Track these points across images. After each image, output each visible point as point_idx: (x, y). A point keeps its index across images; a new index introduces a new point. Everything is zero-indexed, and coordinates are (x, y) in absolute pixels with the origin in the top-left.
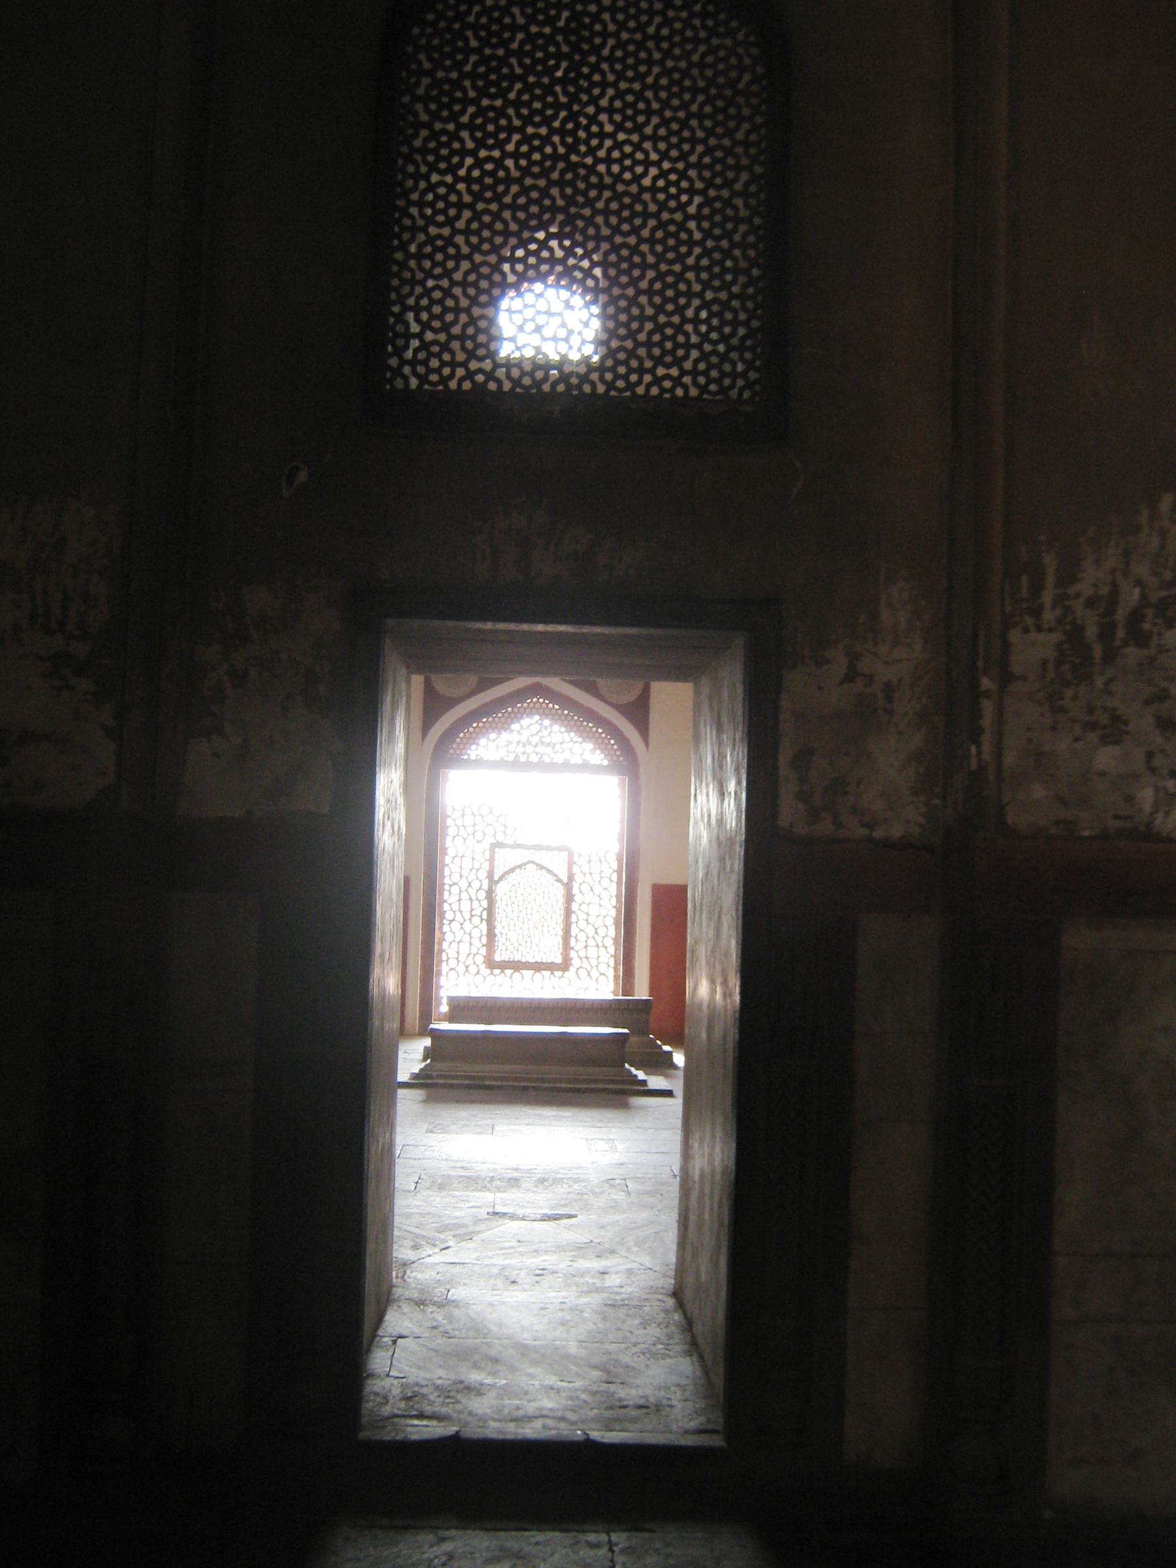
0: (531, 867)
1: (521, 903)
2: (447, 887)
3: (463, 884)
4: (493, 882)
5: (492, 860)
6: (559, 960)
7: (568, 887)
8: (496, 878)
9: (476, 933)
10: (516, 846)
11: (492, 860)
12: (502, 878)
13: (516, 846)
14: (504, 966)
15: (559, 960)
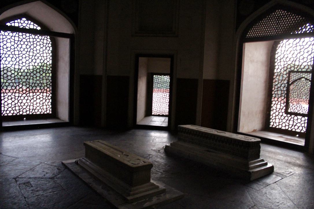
0: (303, 79)
1: (299, 92)
2: (274, 86)
4: (289, 85)
5: (289, 77)
8: (290, 83)
9: (282, 102)
10: (298, 72)
11: (289, 77)
12: (292, 83)
13: (298, 72)
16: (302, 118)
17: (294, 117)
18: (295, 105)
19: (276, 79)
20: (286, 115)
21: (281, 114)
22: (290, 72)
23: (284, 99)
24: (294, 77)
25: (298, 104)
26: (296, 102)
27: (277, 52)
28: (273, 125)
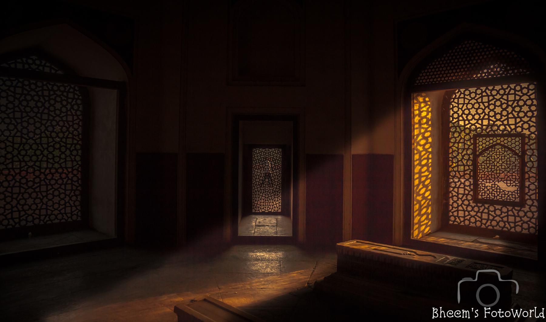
3: (460, 157)
4: (476, 157)
6: (518, 200)
7: (522, 157)
8: (478, 153)
9: (467, 183)
10: (488, 135)
11: (475, 144)
14: (484, 202)
15: (518, 200)
16: (501, 208)
17: (489, 207)
18: (488, 188)
20: (475, 204)
21: (466, 202)
22: (475, 137)
23: (470, 178)
24: (482, 144)
25: (493, 186)
26: (490, 182)
28: (455, 221)
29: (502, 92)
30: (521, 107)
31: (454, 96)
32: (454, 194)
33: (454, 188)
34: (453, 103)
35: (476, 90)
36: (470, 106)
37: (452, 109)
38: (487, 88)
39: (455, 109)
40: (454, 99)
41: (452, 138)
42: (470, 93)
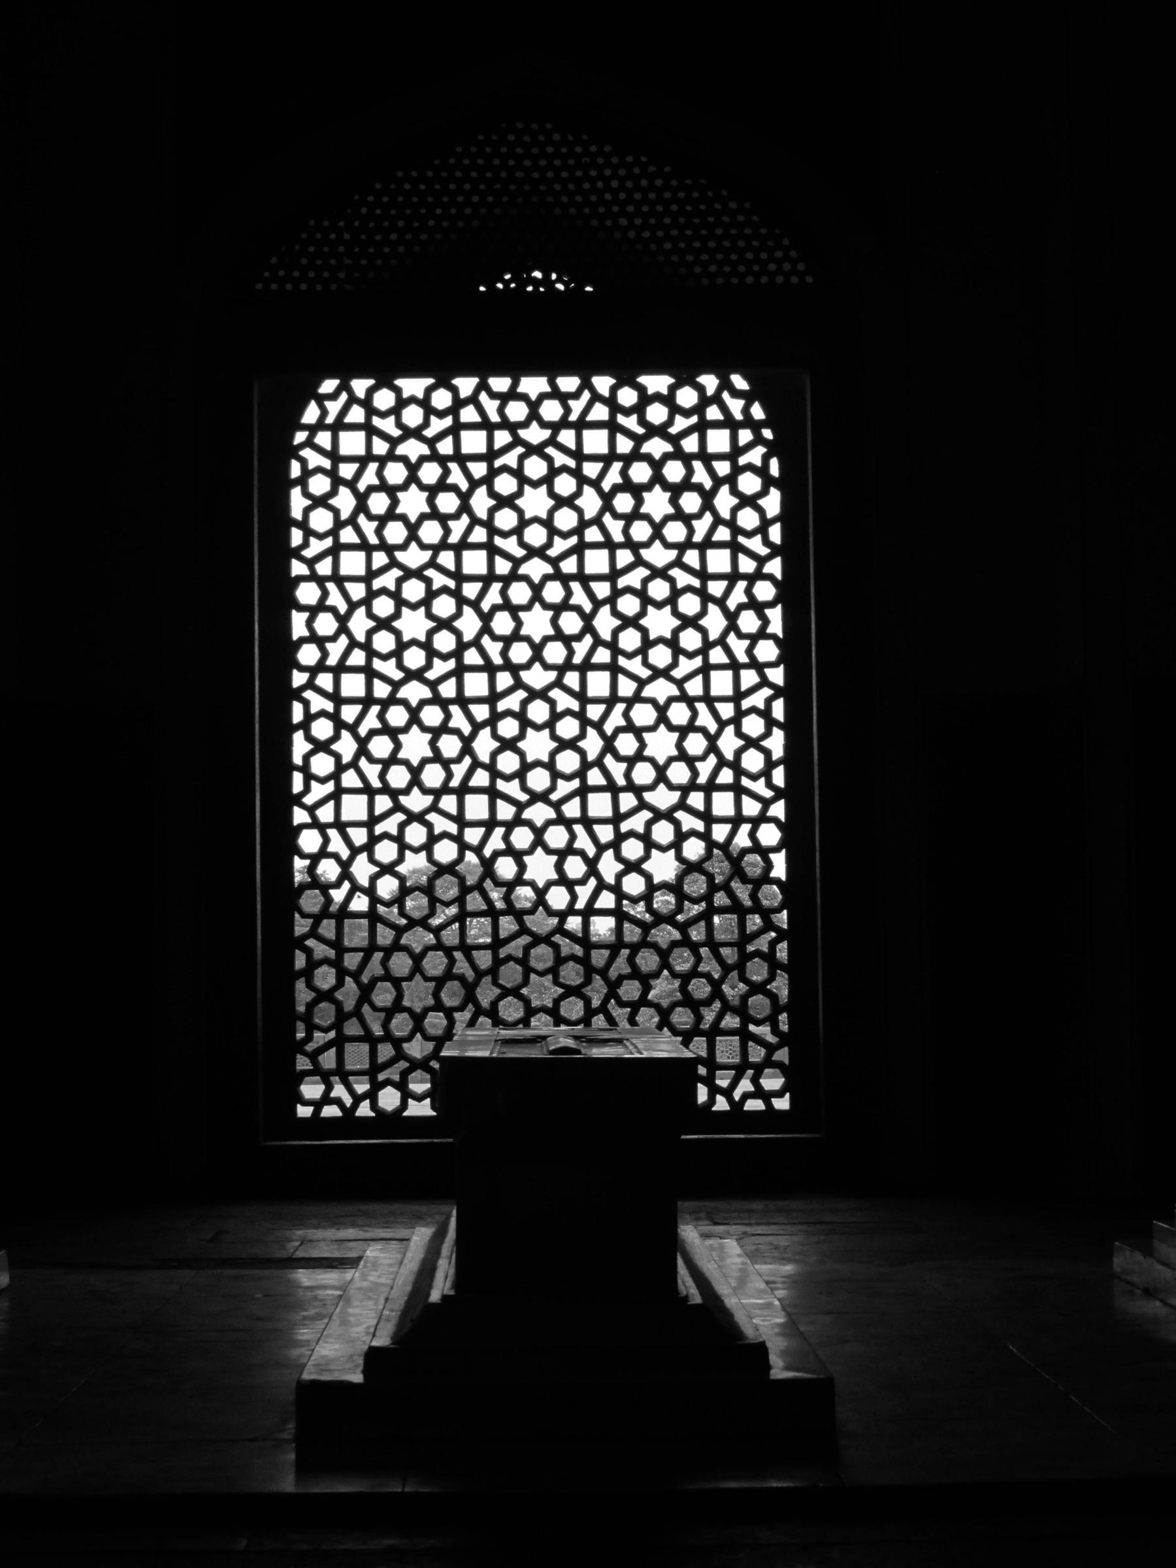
19: (318, 703)
27: (295, 470)
28: (326, 1099)
29: (551, 410)
30: (637, 491)
31: (311, 414)
32: (321, 951)
33: (317, 919)
34: (306, 453)
35: (429, 391)
36: (396, 473)
37: (303, 481)
38: (483, 386)
39: (319, 485)
40: (313, 429)
41: (303, 640)
42: (402, 403)
